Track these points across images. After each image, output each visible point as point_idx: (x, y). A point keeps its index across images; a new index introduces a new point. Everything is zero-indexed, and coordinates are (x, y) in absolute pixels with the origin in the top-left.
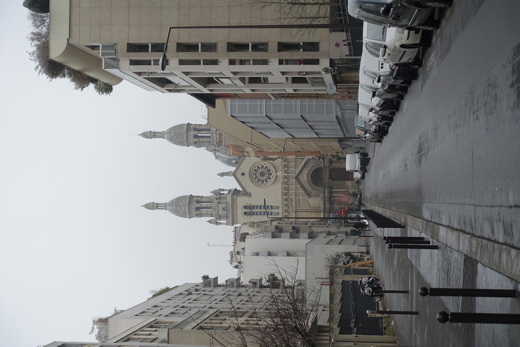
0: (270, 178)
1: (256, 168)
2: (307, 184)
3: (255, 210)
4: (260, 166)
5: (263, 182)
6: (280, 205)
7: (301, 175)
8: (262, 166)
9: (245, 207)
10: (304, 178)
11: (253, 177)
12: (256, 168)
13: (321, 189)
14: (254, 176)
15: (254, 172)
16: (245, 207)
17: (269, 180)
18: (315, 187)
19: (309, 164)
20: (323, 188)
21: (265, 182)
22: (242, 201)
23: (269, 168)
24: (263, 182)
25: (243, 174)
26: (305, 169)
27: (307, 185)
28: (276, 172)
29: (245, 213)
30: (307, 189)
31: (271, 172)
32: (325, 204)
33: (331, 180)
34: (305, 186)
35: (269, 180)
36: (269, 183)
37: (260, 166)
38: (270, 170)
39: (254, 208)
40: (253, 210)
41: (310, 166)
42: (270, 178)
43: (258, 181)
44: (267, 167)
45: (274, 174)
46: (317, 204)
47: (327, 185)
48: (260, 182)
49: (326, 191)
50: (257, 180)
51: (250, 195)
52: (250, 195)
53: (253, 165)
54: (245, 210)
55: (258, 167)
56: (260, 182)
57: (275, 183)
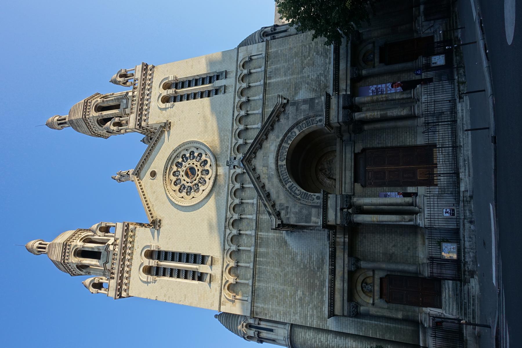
1: (180, 160)
2: (275, 180)
7: (260, 154)
9: (150, 254)
10: (269, 161)
13: (316, 198)
16: (150, 254)
17: (201, 188)
18: (299, 190)
19: (283, 120)
20: (320, 195)
26: (272, 136)
27: (273, 186)
29: (148, 270)
30: (273, 196)
32: (333, 256)
33: (358, 186)
34: (268, 186)
41: (284, 124)
46: (315, 257)
49: (331, 202)
53: (175, 151)
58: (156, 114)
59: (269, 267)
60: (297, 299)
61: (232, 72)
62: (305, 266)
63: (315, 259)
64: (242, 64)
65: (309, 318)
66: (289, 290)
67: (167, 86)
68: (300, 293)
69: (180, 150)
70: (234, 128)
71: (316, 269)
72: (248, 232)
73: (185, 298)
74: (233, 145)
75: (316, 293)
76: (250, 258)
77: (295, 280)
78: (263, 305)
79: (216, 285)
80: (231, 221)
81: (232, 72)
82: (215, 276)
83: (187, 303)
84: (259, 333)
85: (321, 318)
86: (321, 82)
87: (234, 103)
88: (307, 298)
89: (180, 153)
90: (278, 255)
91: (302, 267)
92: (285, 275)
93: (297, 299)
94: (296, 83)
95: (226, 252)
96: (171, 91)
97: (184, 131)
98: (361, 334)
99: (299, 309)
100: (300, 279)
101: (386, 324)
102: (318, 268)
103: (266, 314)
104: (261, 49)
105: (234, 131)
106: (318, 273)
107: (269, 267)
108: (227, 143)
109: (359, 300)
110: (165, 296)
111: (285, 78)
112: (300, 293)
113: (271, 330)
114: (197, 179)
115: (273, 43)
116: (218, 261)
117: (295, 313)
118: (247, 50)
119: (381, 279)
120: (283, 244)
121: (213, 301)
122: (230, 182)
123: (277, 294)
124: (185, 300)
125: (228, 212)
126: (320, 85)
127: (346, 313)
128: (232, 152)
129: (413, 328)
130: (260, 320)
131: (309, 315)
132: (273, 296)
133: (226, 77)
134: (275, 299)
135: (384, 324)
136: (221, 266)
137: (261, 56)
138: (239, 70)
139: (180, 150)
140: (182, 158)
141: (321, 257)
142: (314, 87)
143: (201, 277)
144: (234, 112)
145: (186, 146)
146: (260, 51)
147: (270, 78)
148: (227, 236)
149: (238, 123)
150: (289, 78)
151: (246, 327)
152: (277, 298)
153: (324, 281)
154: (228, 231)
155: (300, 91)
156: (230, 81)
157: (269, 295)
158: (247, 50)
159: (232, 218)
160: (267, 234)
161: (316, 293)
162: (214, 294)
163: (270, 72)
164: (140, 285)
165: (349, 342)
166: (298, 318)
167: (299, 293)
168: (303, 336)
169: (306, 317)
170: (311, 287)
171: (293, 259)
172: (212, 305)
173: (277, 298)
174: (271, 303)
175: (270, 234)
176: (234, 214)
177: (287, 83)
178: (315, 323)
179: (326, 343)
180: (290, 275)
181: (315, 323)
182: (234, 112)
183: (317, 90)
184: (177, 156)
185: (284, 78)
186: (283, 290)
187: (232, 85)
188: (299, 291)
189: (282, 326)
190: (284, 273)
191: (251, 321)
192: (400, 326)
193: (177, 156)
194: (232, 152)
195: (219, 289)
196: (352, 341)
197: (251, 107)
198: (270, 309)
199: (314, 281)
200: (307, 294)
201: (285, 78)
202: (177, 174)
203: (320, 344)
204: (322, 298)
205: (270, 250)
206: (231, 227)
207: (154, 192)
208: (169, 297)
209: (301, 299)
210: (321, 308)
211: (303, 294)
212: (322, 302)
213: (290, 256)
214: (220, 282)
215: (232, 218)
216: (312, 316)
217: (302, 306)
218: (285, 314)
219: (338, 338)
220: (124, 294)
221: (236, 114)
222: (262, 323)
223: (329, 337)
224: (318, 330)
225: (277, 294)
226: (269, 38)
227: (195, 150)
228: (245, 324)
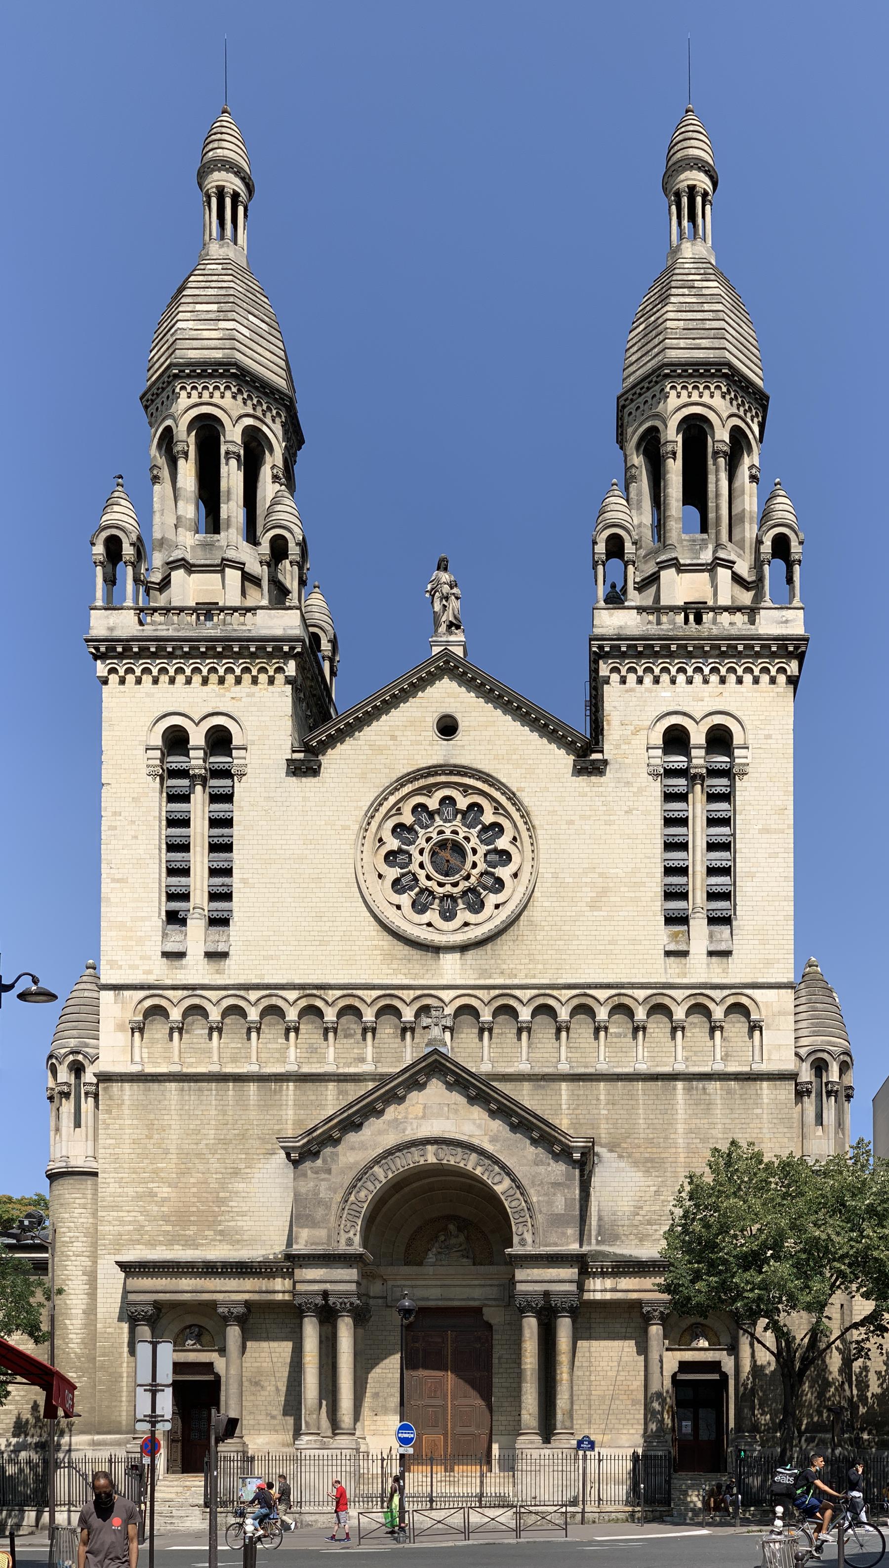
0: (419, 907)
3: (199, 808)
4: (503, 843)
5: (391, 857)
6: (234, 971)
8: (505, 857)
11: (428, 790)
12: (488, 817)
14: (433, 803)
15: (463, 803)
17: (405, 900)
21: (393, 873)
22: (264, 713)
23: (491, 899)
24: (391, 857)
25: (448, 727)
28: (463, 948)
29: (176, 740)
31: (464, 915)
35: (405, 900)
36: (381, 893)
37: (503, 843)
38: (477, 906)
39: (214, 798)
40: (199, 796)
42: (419, 907)
43: (399, 829)
44: (500, 884)
45: (448, 933)
46: (243, 1223)
47: (376, 1288)
48: (393, 844)
50: (407, 818)
51: (304, 766)
52: (304, 766)
53: (512, 797)
54: (197, 737)
55: (497, 829)
56: (393, 844)
57: (387, 941)
58: (636, 709)
59: (214, 1112)
60: (150, 1185)
61: (725, 971)
62: (221, 1202)
63: (239, 1223)
64: (744, 1000)
65: (115, 1214)
66: (169, 1166)
67: (720, 739)
68: (164, 1191)
69: (516, 815)
70: (564, 991)
71: (219, 1228)
72: (292, 1053)
73: (118, 881)
74: (517, 993)
75: (169, 1228)
76: (234, 1060)
77: (192, 1180)
78: (127, 1102)
79: (159, 971)
80: (319, 1003)
81: (725, 971)
82: (182, 967)
83: (107, 887)
84: (67, 1095)
85: (118, 1244)
86: (654, 1227)
87: (633, 986)
88: (156, 1209)
89: (508, 816)
90: (243, 1136)
91: (222, 1195)
92: (200, 1155)
93: (150, 1185)
94: (663, 1161)
95: (242, 993)
96: (699, 759)
97: (571, 822)
98: (99, 1326)
99: (130, 1191)
100: (195, 1190)
101: (125, 1375)
102: (221, 1233)
103: (109, 1112)
104: (775, 1056)
105: (555, 993)
106: (212, 1233)
107: (214, 1112)
108: (522, 975)
109: (163, 1321)
110: (115, 814)
111: (681, 1131)
112: (164, 1191)
113: (78, 1124)
114: (429, 884)
115: (787, 1090)
116: (218, 972)
117: (120, 1181)
118: (781, 1013)
119: (210, 1365)
120: (269, 1146)
121: (120, 967)
122: (419, 992)
123: (156, 1136)
124: (114, 880)
125: (339, 993)
126: (649, 1223)
127: (132, 1297)
128: (497, 992)
129: (124, 1423)
130: (96, 1096)
131: (121, 1214)
132: (150, 1126)
133: (711, 954)
134: (146, 1132)
135: (124, 1369)
136: (206, 981)
137: (757, 1057)
138: (727, 992)
139: (516, 815)
140: (495, 825)
141: (245, 1237)
142: (646, 1208)
143: (174, 918)
144: (608, 986)
145: (525, 834)
146: (769, 1054)
147: (688, 1090)
148: (280, 993)
149: (576, 1002)
150: (680, 1141)
151: (75, 1062)
152: (149, 1137)
153: (196, 1246)
154: (292, 995)
155: (641, 1174)
156: (699, 969)
157: (152, 1116)
158: (781, 1013)
159: (327, 1002)
160: (291, 1103)
161: (169, 1228)
162: (136, 967)
163: (704, 1089)
164: (133, 713)
165: (80, 1302)
166: (113, 1190)
167: (165, 1190)
168: (77, 1201)
169: (116, 1207)
170: (181, 1218)
171: (236, 1173)
172: (113, 964)
173: (149, 1137)
174: (135, 1122)
175: (291, 1112)
176: (336, 1009)
177: (666, 1138)
178: (107, 1228)
179: (71, 1253)
180: (201, 1167)
181: (107, 1228)
182: (608, 986)
183: (638, 1218)
184: (498, 807)
185: (681, 1128)
186: (167, 1152)
187: (685, 975)
188: (169, 1190)
189: (90, 1153)
190: (204, 1151)
191: (89, 1077)
192: (124, 1399)
193: (498, 807)
194: (497, 992)
195: (151, 979)
196: (84, 1307)
197: (618, 1035)
198: (121, 1122)
199: (194, 1223)
200: (165, 1209)
201: (681, 1131)
202: (448, 811)
203: (67, 1239)
204: (161, 1243)
205: (253, 1114)
206: (303, 1003)
207: (394, 738)
208: (115, 828)
209: (152, 1194)
210: (138, 1242)
211: (164, 1200)
212: (152, 1244)
213: (243, 1166)
214: (169, 982)
215: (327, 1002)
216: (122, 1222)
217: (139, 1197)
218: (116, 1159)
219: (85, 1278)
220: (101, 669)
221: (602, 995)
222: (91, 1100)
223: (83, 1259)
224: (94, 1238)
225: (156, 1136)
226: (806, 1075)
227: (512, 868)
228: (80, 1057)
